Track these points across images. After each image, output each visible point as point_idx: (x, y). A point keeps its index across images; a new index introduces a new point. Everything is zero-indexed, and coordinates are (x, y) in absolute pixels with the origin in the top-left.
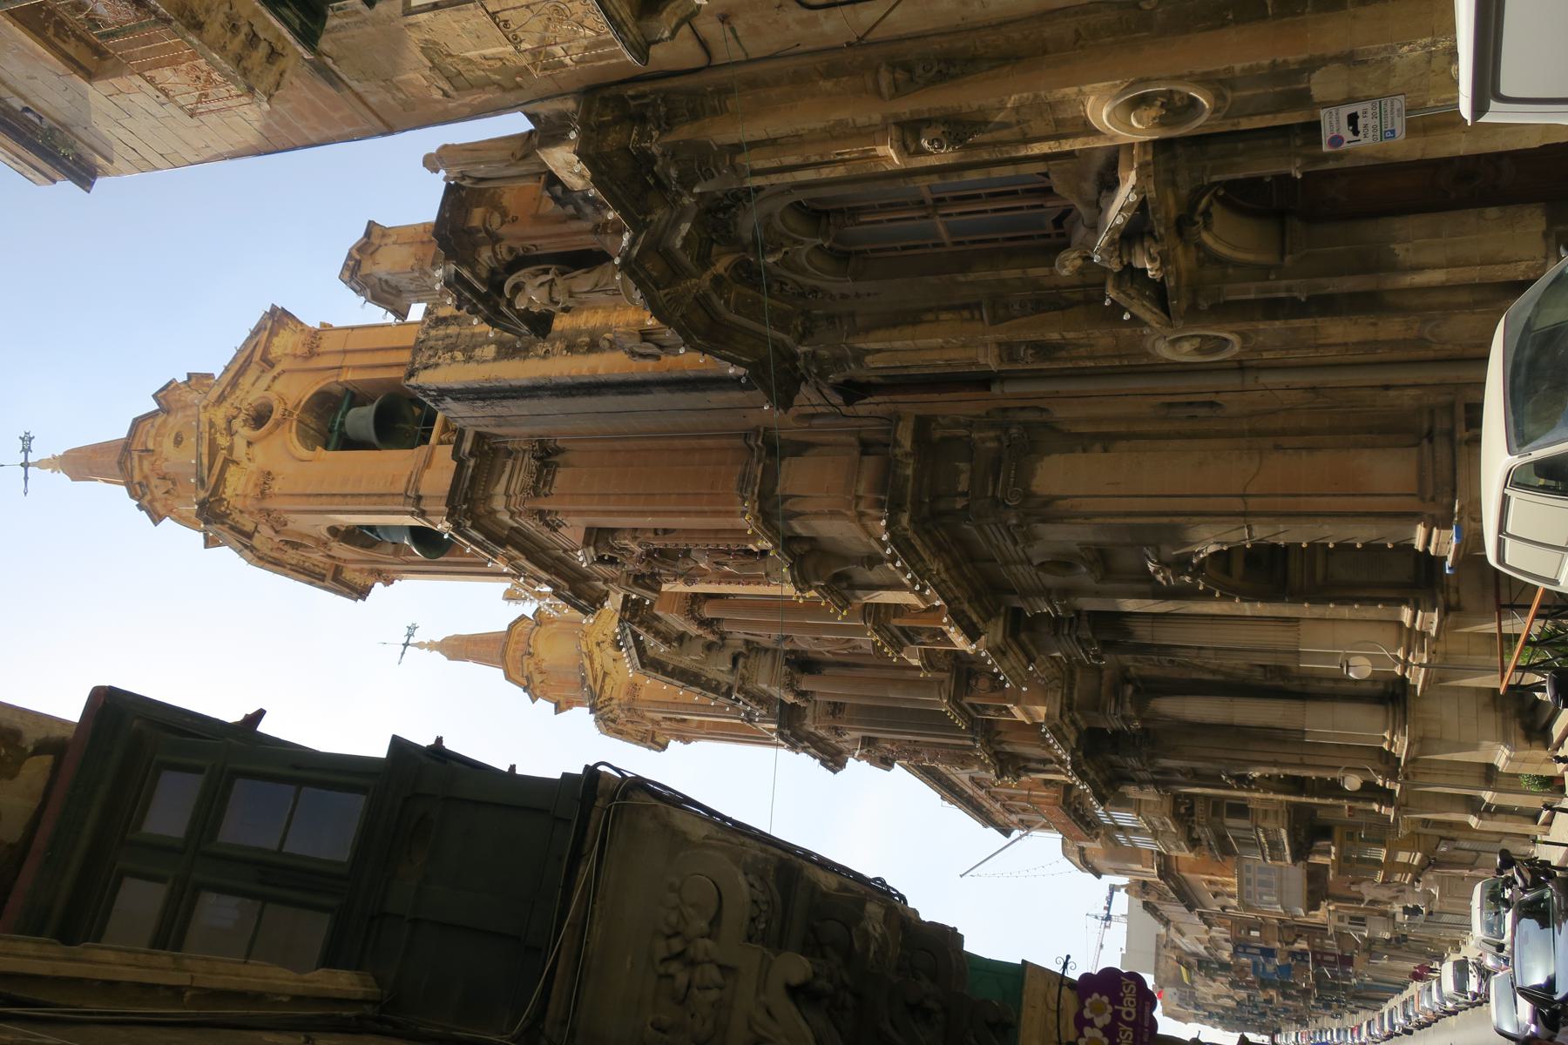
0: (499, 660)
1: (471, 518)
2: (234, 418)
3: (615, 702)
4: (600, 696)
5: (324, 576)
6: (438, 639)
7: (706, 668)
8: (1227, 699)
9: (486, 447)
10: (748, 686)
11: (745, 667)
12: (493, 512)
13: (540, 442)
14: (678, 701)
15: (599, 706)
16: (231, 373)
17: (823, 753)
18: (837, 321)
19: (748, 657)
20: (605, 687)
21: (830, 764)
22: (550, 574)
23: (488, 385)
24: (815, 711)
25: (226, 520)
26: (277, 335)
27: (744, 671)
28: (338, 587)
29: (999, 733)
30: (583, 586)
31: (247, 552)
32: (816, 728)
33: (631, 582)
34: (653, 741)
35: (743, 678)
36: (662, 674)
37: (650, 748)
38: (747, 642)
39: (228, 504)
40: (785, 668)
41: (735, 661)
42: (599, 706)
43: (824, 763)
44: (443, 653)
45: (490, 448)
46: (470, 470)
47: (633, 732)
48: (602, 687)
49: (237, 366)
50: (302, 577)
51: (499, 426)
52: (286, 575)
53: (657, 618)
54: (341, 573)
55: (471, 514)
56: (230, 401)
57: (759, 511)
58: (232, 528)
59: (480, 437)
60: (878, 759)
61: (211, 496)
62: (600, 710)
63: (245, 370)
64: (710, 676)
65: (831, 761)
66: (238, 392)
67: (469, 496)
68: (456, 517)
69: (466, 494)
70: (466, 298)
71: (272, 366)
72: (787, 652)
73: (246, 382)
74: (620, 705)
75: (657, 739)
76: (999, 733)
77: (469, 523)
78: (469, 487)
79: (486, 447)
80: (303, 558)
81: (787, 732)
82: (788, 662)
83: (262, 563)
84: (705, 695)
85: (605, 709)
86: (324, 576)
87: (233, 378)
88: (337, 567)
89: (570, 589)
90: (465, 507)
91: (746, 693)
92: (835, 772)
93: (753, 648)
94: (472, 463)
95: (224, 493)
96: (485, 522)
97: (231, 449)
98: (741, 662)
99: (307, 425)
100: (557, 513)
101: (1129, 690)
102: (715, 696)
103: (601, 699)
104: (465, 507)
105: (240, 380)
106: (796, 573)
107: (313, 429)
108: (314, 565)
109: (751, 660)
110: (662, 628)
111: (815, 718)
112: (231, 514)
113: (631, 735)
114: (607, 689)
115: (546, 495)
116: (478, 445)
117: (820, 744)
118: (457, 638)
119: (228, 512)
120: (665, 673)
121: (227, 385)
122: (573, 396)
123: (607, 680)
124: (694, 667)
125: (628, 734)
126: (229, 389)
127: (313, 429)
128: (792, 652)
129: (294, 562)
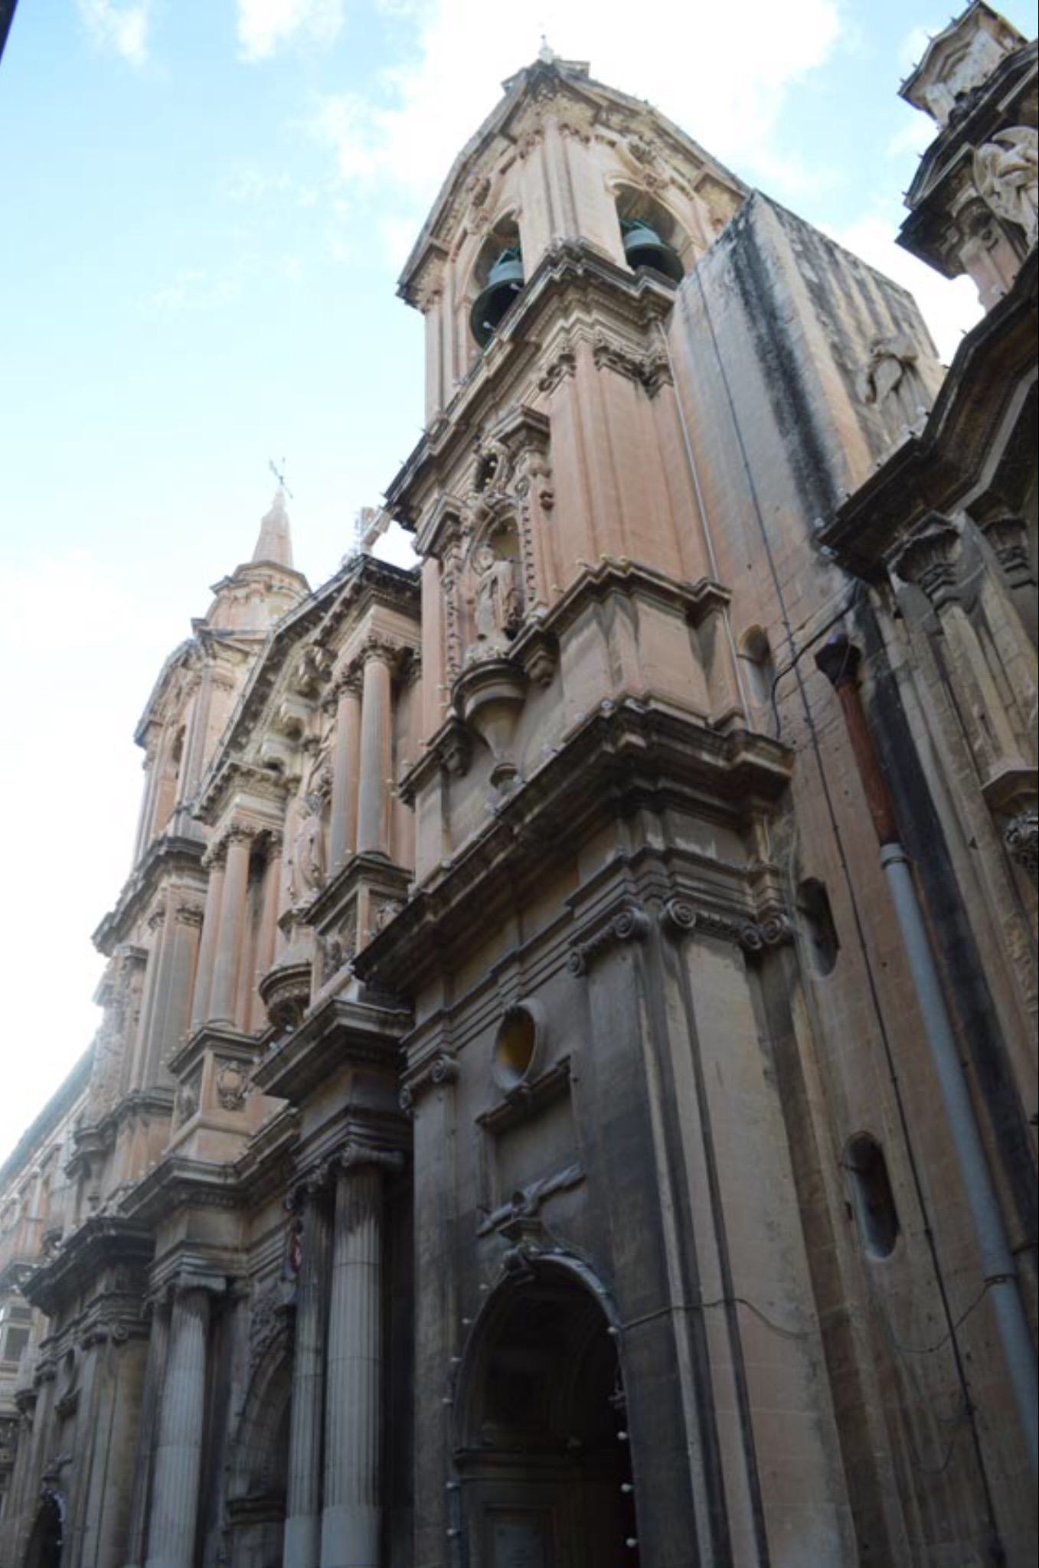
0: (263, 558)
1: (563, 281)
2: (641, 138)
3: (211, 662)
4: (220, 644)
5: (437, 237)
6: (289, 509)
7: (265, 728)
8: (197, 1435)
9: (652, 315)
10: (238, 780)
12: (566, 312)
13: (665, 368)
14: (209, 730)
16: (688, 146)
17: (124, 913)
18: (1018, 561)
19: (276, 784)
21: (106, 927)
22: (458, 424)
23: (769, 265)
24: (188, 887)
25: (529, 96)
26: (732, 200)
27: (258, 777)
28: (422, 251)
29: (146, 1125)
30: (432, 478)
31: (478, 142)
32: (164, 889)
33: (450, 509)
34: (151, 723)
35: (249, 774)
37: (141, 722)
38: (297, 780)
39: (551, 99)
40: (258, 829)
41: (274, 766)
43: (110, 917)
44: (271, 512)
45: (650, 320)
46: (624, 288)
47: (163, 700)
48: (229, 647)
49: (696, 153)
50: (436, 215)
51: (687, 320)
52: (440, 197)
53: (363, 611)
54: (439, 258)
55: (570, 275)
56: (656, 140)
57: (611, 576)
58: (517, 106)
59: (665, 308)
60: (111, 982)
61: (561, 81)
62: (203, 643)
63: (691, 162)
64: (254, 735)
65: (111, 928)
66: (667, 152)
67: (593, 281)
68: (566, 259)
69: (596, 277)
70: (981, 98)
71: (697, 189)
72: (280, 832)
73: (678, 161)
74: (207, 666)
76: (146, 1125)
77: (557, 276)
78: (604, 283)
79: (652, 315)
80: (459, 215)
82: (267, 834)
83: (458, 167)
84: (228, 727)
85: (202, 651)
86: (437, 237)
87: (684, 148)
88: (446, 254)
89: (431, 457)
90: (580, 272)
91: (227, 779)
92: (94, 937)
93: (286, 788)
94: (635, 293)
95: (564, 96)
96: (554, 303)
97: (606, 125)
98: (272, 774)
99: (635, 204)
100: (572, 375)
101: (218, 1285)
102: (226, 742)
104: (580, 272)
105: (680, 156)
106: (491, 667)
107: (629, 212)
108: (449, 230)
109: (272, 789)
110: (345, 626)
111: (179, 887)
112: (536, 101)
113: (161, 697)
114: (228, 654)
115: (597, 363)
116: (655, 304)
117: (138, 907)
118: (286, 528)
119: (540, 98)
121: (676, 140)
122: (763, 359)
123: (239, 657)
124: (268, 711)
125: (161, 697)
126: (671, 141)
127: (629, 212)
128: (280, 841)
129: (456, 206)
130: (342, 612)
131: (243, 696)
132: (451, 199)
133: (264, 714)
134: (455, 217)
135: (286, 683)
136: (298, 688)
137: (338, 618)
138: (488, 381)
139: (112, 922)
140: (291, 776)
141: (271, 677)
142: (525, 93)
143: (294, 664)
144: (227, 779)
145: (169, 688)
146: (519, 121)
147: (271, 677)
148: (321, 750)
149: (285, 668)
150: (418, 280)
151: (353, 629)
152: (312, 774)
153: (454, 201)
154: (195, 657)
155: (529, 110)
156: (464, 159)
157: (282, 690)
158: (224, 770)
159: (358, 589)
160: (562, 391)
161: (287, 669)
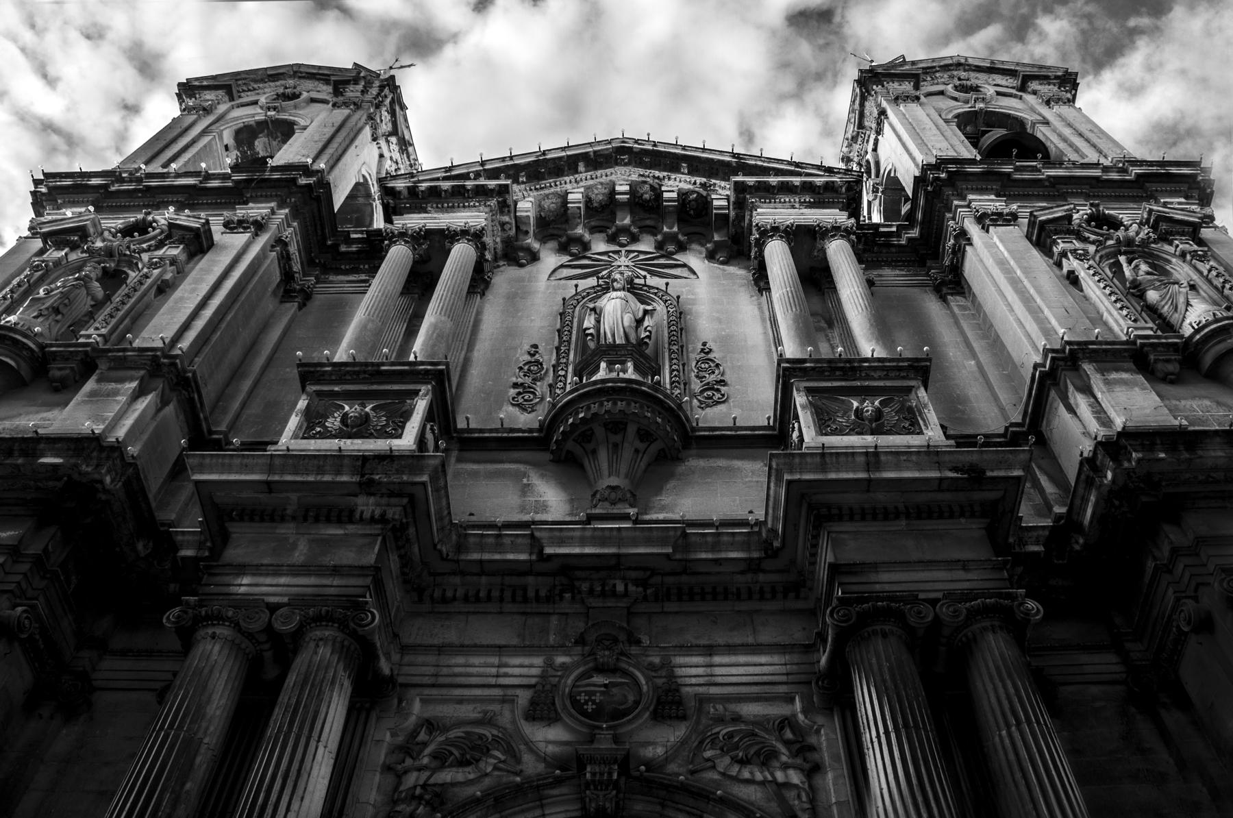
7: (536, 193)
10: (493, 202)
11: (503, 224)
15: (386, 91)
20: (389, 117)
22: (1049, 177)
27: (506, 219)
36: (587, 153)
38: (534, 257)
42: (386, 91)
54: (914, 86)
65: (105, 187)
75: (221, 93)
80: (936, 81)
81: (303, 181)
85: (374, 91)
91: (481, 192)
103: (388, 101)
109: (498, 240)
114: (386, 116)
120: (584, 157)
129: (938, 75)
130: (797, 186)
131: (544, 153)
132: (938, 69)
133: (543, 183)
134: (933, 79)
135: (591, 182)
136: (593, 196)
137: (787, 188)
138: (1097, 179)
139: (113, 183)
140: (525, 246)
141: (581, 167)
142: (1057, 77)
143: (613, 178)
144: (481, 192)
145: (272, 84)
146: (1041, 84)
147: (581, 167)
148: (585, 257)
149: (599, 173)
150: (888, 79)
151: (793, 207)
152: (562, 266)
153: (938, 71)
154: (360, 87)
155: (1051, 87)
156: (963, 61)
157: (581, 184)
158: (492, 183)
159: (829, 187)
160: (240, 239)
161: (604, 176)
